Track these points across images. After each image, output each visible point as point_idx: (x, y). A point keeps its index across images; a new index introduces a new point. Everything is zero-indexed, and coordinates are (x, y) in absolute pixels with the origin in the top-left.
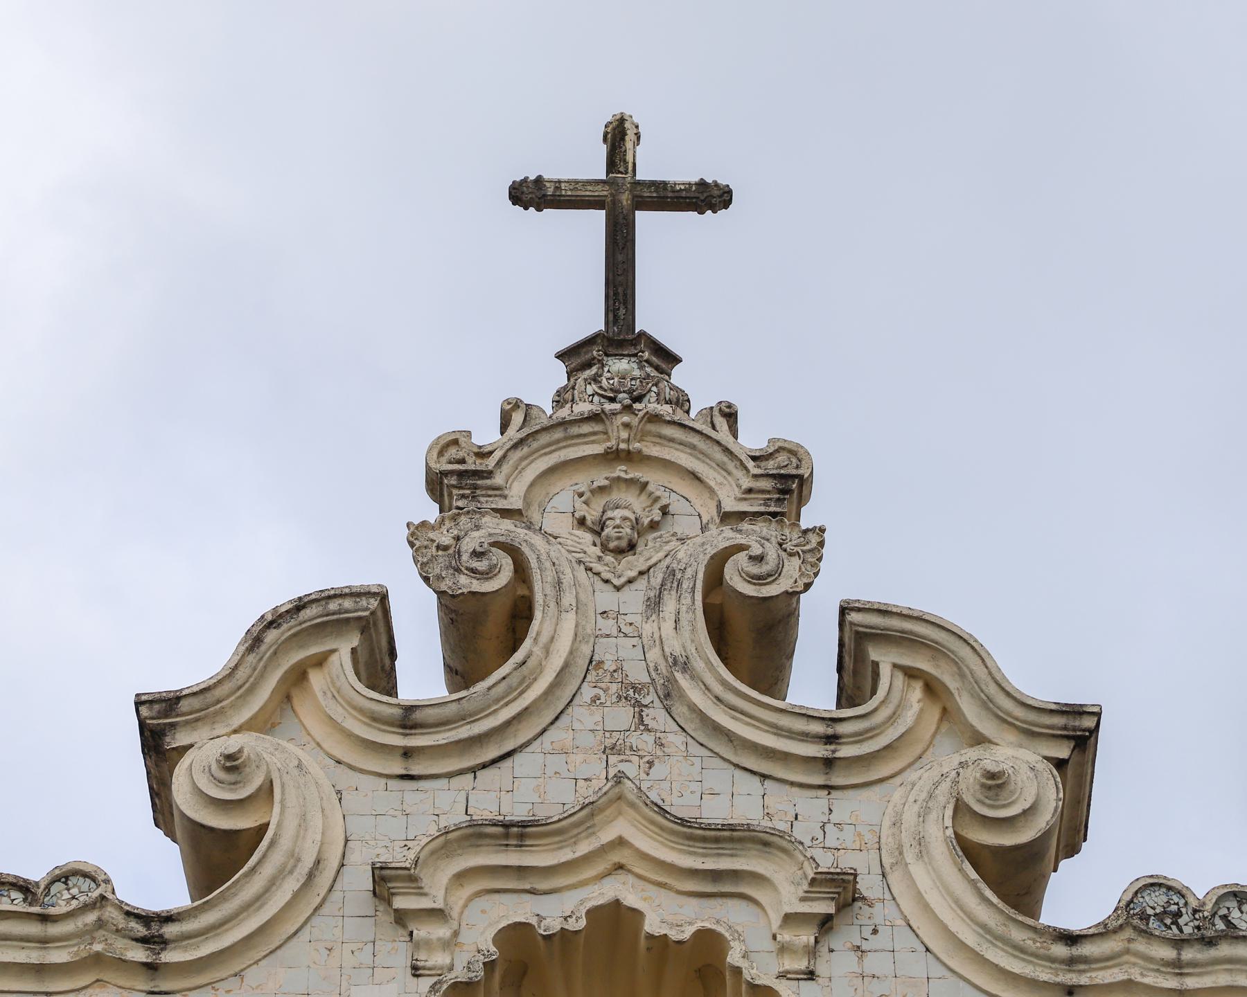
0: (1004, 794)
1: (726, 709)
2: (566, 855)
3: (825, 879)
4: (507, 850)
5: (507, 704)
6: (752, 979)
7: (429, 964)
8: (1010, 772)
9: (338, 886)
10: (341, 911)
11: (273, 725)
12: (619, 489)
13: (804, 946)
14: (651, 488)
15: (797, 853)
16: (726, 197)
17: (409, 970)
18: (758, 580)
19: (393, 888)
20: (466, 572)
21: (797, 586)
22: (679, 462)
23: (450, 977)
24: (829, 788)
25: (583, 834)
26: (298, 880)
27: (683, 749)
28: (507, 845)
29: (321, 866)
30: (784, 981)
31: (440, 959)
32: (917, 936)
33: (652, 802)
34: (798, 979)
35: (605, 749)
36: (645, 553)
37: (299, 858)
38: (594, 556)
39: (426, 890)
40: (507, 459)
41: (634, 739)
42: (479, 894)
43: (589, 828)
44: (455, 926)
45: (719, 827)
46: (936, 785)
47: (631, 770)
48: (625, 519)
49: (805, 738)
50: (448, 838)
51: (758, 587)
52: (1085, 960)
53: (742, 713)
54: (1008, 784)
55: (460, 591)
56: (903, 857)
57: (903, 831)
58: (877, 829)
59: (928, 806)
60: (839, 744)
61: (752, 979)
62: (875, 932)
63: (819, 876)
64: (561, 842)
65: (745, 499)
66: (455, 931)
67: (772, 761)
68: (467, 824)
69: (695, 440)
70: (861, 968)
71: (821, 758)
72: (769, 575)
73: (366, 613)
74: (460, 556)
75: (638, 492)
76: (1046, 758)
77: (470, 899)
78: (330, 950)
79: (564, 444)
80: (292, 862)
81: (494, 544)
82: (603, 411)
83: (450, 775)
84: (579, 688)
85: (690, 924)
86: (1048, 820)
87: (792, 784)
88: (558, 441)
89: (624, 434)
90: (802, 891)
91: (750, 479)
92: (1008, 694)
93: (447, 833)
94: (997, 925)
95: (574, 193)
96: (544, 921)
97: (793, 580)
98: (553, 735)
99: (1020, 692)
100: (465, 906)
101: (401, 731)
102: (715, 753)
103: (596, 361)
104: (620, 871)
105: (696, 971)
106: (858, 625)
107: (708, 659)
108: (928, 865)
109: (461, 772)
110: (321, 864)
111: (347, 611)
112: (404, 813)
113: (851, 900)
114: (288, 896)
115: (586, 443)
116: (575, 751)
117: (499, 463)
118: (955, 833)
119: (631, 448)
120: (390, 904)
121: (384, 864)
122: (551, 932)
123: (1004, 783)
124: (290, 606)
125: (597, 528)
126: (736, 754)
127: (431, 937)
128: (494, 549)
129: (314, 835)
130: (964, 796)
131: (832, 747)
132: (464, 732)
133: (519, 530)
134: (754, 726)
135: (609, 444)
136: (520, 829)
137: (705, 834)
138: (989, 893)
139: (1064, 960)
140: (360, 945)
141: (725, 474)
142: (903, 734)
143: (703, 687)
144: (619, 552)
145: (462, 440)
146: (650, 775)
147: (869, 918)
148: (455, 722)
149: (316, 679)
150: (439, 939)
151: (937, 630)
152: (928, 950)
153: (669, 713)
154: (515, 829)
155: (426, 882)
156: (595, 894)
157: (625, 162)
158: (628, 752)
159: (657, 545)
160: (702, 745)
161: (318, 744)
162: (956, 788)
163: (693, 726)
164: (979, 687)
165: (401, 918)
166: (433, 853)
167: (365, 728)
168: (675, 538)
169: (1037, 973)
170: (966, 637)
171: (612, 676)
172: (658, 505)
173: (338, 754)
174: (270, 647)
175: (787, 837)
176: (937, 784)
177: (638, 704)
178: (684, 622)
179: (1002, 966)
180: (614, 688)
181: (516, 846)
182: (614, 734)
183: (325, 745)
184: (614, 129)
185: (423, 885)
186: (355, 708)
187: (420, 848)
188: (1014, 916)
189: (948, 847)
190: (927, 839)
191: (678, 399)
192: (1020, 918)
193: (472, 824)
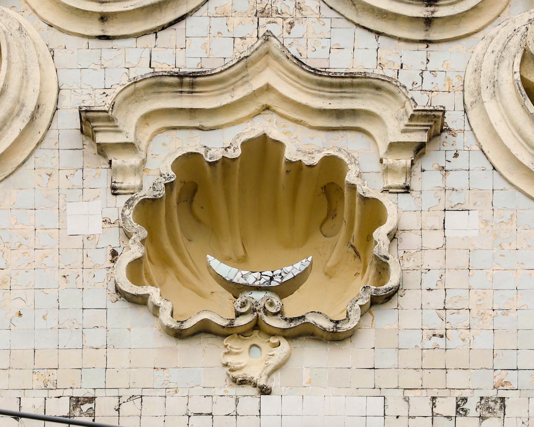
2: (226, 99)
4: (181, 96)
6: (364, 193)
7: (124, 185)
13: (403, 168)
15: (401, 95)
17: (109, 190)
19: (96, 127)
23: (140, 196)
25: (240, 82)
27: (317, 12)
28: (181, 92)
29: (40, 110)
30: (387, 194)
35: (257, 13)
39: (120, 128)
42: (160, 131)
43: (244, 77)
46: (510, 38)
47: (276, 30)
50: (136, 87)
56: (481, 97)
57: (482, 75)
58: (462, 75)
59: (502, 55)
61: (364, 193)
62: (456, 155)
68: (151, 75)
85: (319, 152)
90: (403, 125)
93: (136, 82)
96: (210, 151)
102: (342, 15)
105: (322, 188)
108: (499, 102)
113: (439, 131)
114: (16, 134)
116: (233, 14)
118: (522, 77)
120: (93, 139)
121: (88, 108)
122: (215, 160)
127: (125, 165)
129: (34, 85)
130: (530, 47)
136: (191, 79)
146: (291, 34)
150: (131, 166)
154: (187, 79)
155: (120, 122)
156: (248, 130)
158: (274, 15)
160: (331, 8)
162: (524, 40)
166: (125, 98)
176: (510, 38)
181: (189, 92)
185: (118, 124)
187: (116, 95)
189: (515, 89)
190: (500, 82)
193: (155, 76)
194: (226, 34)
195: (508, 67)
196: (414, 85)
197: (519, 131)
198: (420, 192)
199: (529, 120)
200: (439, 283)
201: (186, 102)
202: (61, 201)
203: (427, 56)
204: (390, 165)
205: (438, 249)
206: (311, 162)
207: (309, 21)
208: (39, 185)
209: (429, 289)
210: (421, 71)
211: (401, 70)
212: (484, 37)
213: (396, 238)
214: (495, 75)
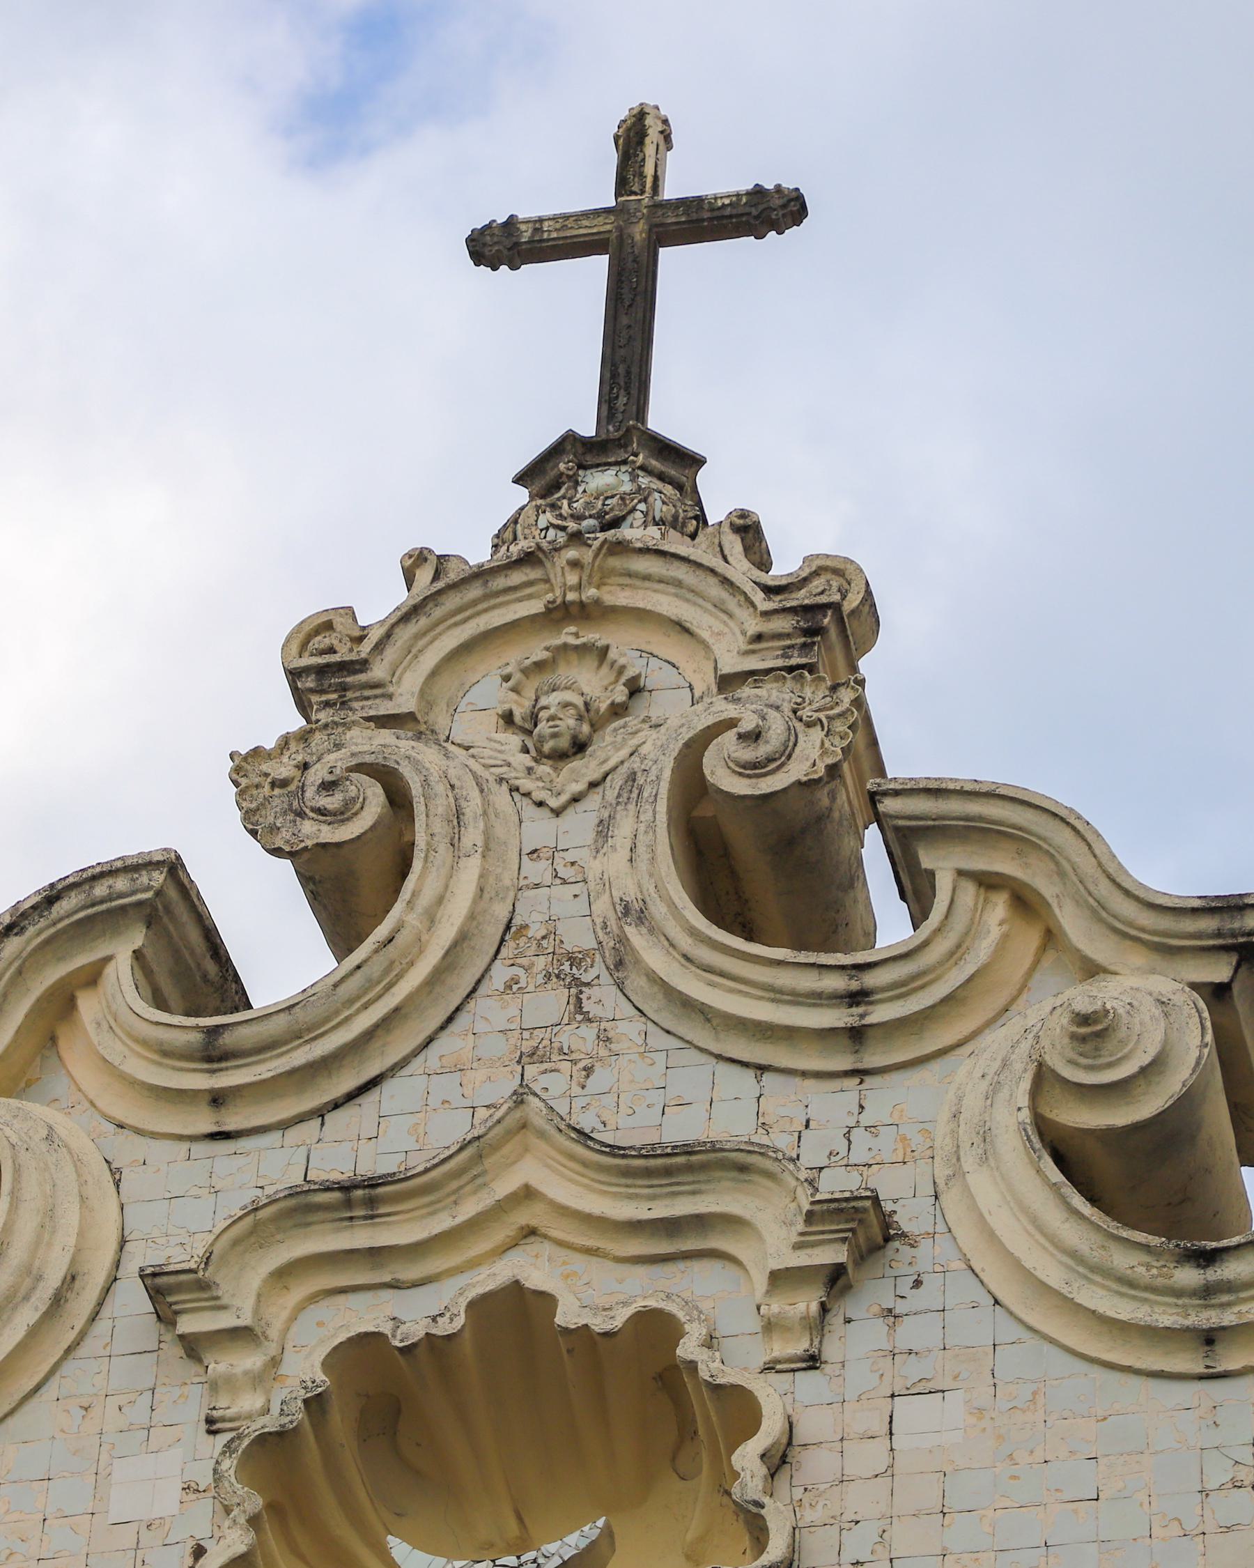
0: (1110, 1045)
1: (699, 971)
2: (442, 1223)
3: (828, 1211)
4: (352, 1226)
5: (366, 1007)
6: (712, 1376)
7: (229, 1413)
8: (1121, 1011)
9: (106, 1312)
10: (108, 1348)
11: (29, 1084)
12: (568, 662)
13: (801, 1319)
14: (612, 654)
16: (794, 207)
17: (203, 1427)
18: (753, 768)
19: (176, 1303)
20: (311, 815)
21: (815, 772)
22: (659, 609)
23: (255, 1427)
24: (860, 1074)
25: (468, 1188)
26: (36, 1309)
27: (640, 1041)
28: (351, 1218)
30: (772, 1376)
31: (250, 1402)
32: (982, 1282)
33: (569, 1126)
34: (793, 1371)
35: (521, 1057)
36: (599, 753)
37: (41, 1276)
38: (521, 768)
39: (224, 1301)
40: (392, 640)
41: (566, 1037)
43: (476, 1177)
44: (272, 1349)
45: (669, 1150)
48: (566, 705)
49: (819, 1002)
50: (257, 1218)
51: (754, 780)
52: (1228, 1287)
53: (722, 974)
54: (1114, 1030)
55: (302, 845)
57: (962, 1122)
60: (871, 1003)
61: (712, 1376)
63: (817, 1207)
64: (432, 1203)
65: (753, 652)
66: (273, 1359)
67: (771, 1043)
68: (286, 1193)
69: (679, 571)
70: (892, 1343)
71: (843, 1028)
72: (770, 760)
73: (149, 895)
74: (303, 791)
75: (596, 664)
76: (1194, 986)
77: (301, 1308)
78: (86, 1409)
79: (484, 605)
80: (28, 1282)
81: (359, 768)
82: (539, 547)
83: (284, 1125)
84: (488, 969)
85: (625, 1304)
86: (1185, 1078)
87: (804, 1074)
88: (474, 603)
89: (572, 579)
91: (759, 618)
92: (1127, 893)
93: (256, 1209)
94: (1091, 1248)
95: (562, 234)
96: (402, 1327)
97: (809, 763)
98: (447, 1044)
99: (1145, 887)
100: (293, 1318)
101: (206, 1066)
102: (687, 1042)
103: (564, 479)
104: (532, 1239)
106: (897, 817)
107: (670, 898)
109: (301, 1119)
110: (77, 1282)
111: (121, 895)
112: (212, 1190)
113: (880, 1240)
115: (520, 600)
116: (475, 1065)
117: (379, 647)
119: (584, 598)
121: (158, 1268)
122: (409, 1343)
123: (1106, 1029)
124: (38, 898)
125: (528, 726)
126: (717, 1040)
127: (234, 1371)
128: (354, 776)
131: (860, 1010)
132: (301, 1056)
133: (402, 743)
134: (740, 992)
135: (550, 596)
136: (367, 1191)
137: (649, 1164)
138: (1078, 1201)
139: (1195, 1289)
140: (132, 1397)
141: (725, 618)
142: (973, 976)
143: (666, 943)
144: (560, 756)
145: (338, 622)
146: (586, 1089)
147: (910, 1263)
148: (286, 1043)
149: (88, 1005)
150: (246, 1373)
151: (1019, 809)
152: (997, 1302)
153: (621, 990)
155: (224, 1290)
157: (642, 176)
158: (555, 1057)
159: (619, 738)
160: (668, 1032)
161: (92, 1104)
163: (655, 1006)
164: (1086, 888)
165: (193, 1347)
166: (236, 1243)
167: (153, 1068)
168: (646, 726)
169: (1155, 1317)
170: (1063, 813)
171: (539, 945)
172: (623, 679)
173: (120, 1114)
174: (11, 964)
175: (771, 1154)
177: (577, 983)
178: (641, 849)
179: (1101, 1311)
180: (541, 962)
181: (365, 1218)
182: (536, 1032)
183: (99, 1103)
184: (629, 130)
185: (220, 1293)
186: (136, 1040)
187: (214, 1237)
188: (1115, 1232)
190: (994, 1131)
191: (676, 517)
192: (1125, 1233)
194: (458, 1101)
195: (1009, 1101)
196: (832, 1157)
197: (1034, 1220)
198: (841, 1365)
199: (1052, 1196)
200: (879, 1548)
201: (362, 1237)
202: (104, 1457)
203: (860, 1099)
204: (773, 1316)
205: (877, 1476)
206: (608, 1326)
207: (623, 1060)
208: (62, 1431)
209: (855, 1561)
210: (848, 1129)
211: (808, 1131)
212: (973, 1052)
213: (788, 1463)
214: (987, 1119)
